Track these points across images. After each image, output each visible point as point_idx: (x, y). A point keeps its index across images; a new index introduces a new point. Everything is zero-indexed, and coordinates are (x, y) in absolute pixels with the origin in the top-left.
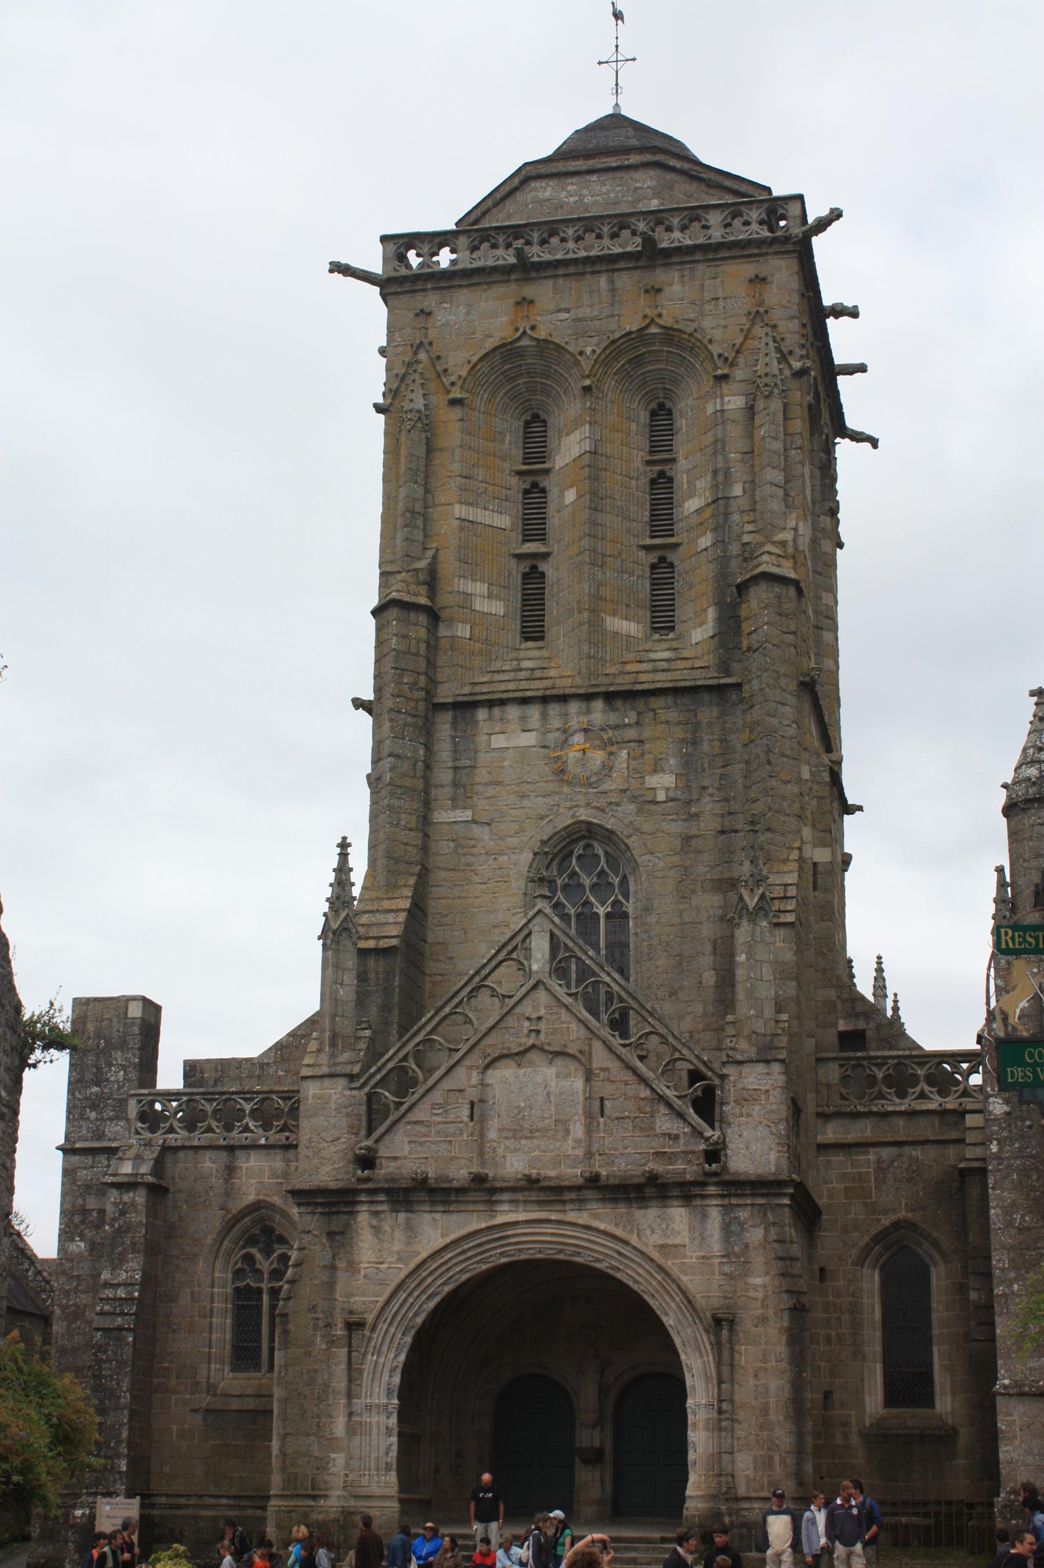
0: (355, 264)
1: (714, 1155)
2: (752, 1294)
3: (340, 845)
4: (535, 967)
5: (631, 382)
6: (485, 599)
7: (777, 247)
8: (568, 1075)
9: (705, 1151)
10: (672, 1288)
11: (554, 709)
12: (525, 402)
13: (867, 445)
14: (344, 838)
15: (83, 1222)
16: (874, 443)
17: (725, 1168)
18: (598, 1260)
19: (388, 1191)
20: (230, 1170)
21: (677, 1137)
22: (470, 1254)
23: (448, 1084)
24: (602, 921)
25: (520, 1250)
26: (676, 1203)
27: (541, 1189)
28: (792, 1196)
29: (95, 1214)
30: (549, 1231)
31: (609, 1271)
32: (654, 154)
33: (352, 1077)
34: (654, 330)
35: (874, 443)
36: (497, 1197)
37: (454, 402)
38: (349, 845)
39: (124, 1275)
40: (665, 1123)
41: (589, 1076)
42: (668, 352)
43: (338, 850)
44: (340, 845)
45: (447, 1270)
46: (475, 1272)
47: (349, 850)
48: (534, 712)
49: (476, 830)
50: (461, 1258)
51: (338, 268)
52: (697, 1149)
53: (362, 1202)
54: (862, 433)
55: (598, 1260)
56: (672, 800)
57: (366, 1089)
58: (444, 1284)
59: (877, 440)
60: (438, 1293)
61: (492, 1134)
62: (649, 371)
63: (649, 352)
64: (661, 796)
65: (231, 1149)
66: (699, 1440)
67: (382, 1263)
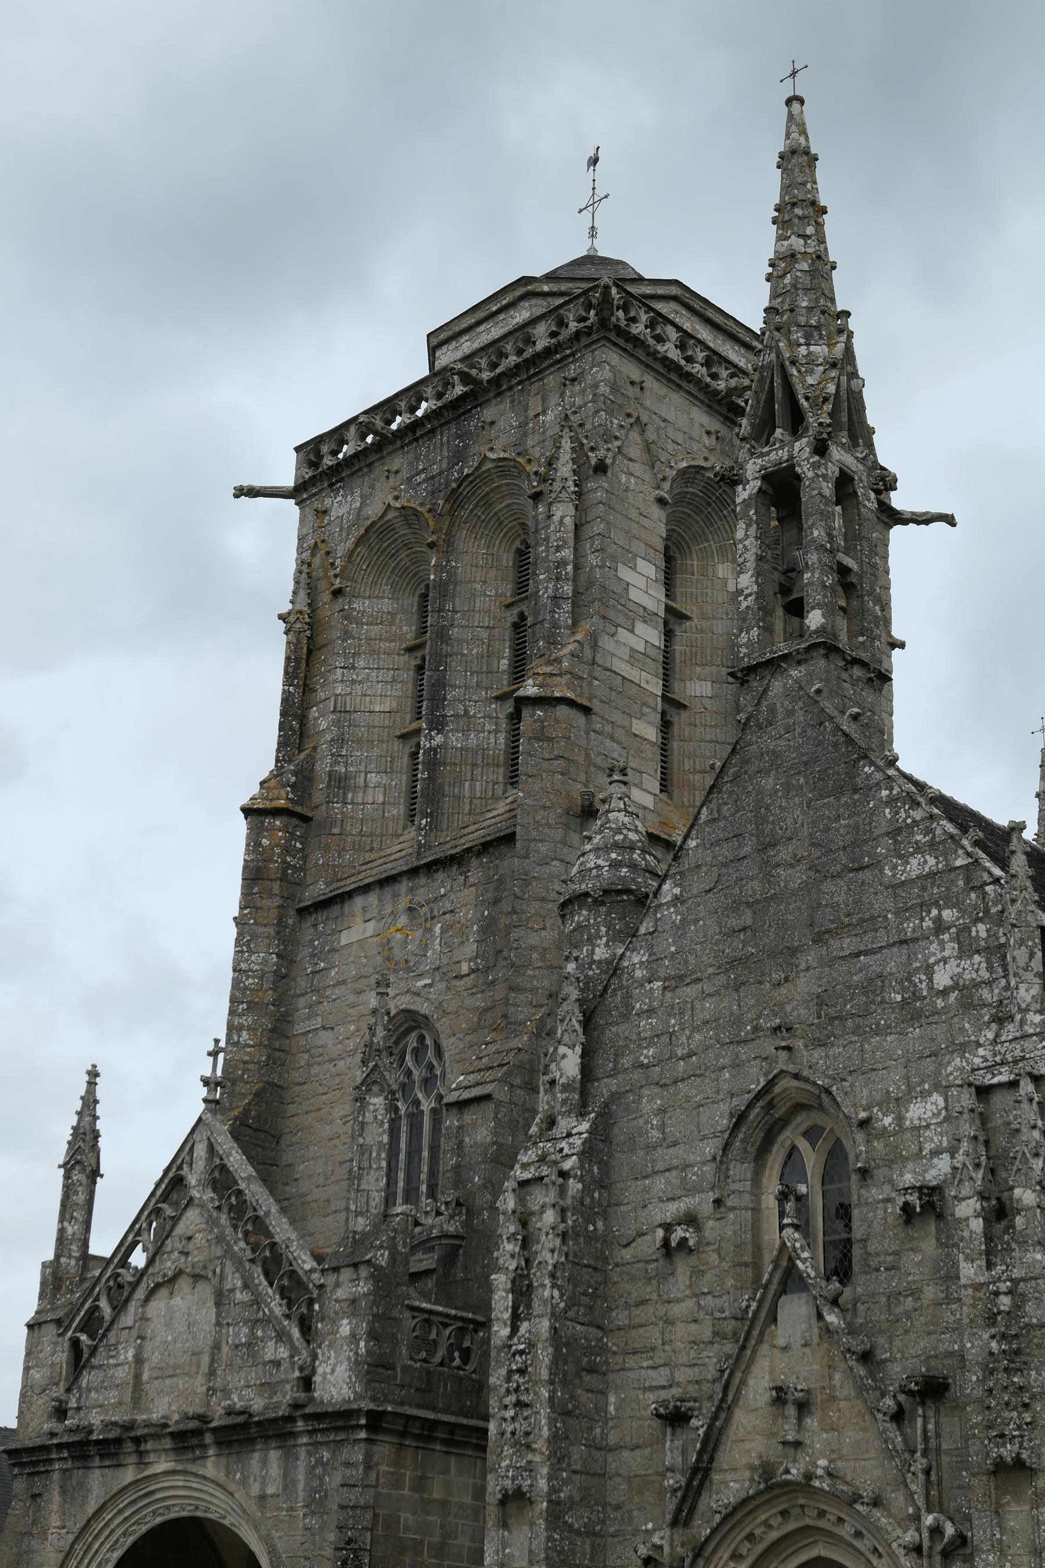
0: (258, 483)
1: (307, 1383)
3: (89, 1073)
5: (486, 527)
6: (377, 789)
7: (584, 341)
9: (299, 1378)
11: (388, 892)
12: (415, 574)
13: (942, 525)
14: (94, 1066)
16: (950, 520)
17: (311, 1400)
19: (67, 1445)
21: (277, 1363)
22: (127, 1514)
24: (426, 1118)
25: (168, 1508)
26: (274, 1445)
27: (172, 1435)
28: (368, 1427)
30: (180, 1484)
32: (526, 285)
33: (58, 1322)
34: (488, 466)
35: (950, 520)
36: (143, 1447)
37: (337, 593)
38: (97, 1075)
41: (221, 1298)
42: (508, 484)
43: (87, 1078)
44: (89, 1073)
45: (113, 1531)
46: (137, 1535)
47: (98, 1080)
48: (372, 898)
49: (326, 1037)
50: (120, 1518)
51: (241, 492)
52: (291, 1376)
53: (52, 1460)
54: (925, 514)
56: (474, 971)
57: (69, 1334)
58: (112, 1549)
59: (953, 516)
60: (108, 1561)
61: (145, 1377)
62: (500, 510)
63: (493, 490)
64: (465, 968)
67: (64, 1527)
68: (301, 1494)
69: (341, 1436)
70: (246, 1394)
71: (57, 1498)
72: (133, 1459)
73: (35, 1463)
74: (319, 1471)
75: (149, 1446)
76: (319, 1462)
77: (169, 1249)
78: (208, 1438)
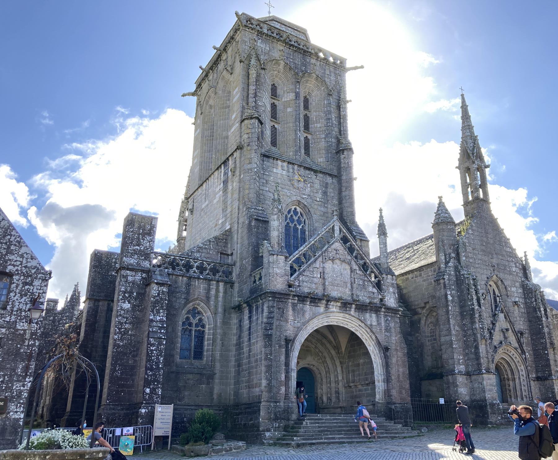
1: (381, 300)
2: (393, 342)
4: (336, 236)
8: (346, 270)
10: (374, 337)
15: (129, 296)
18: (353, 327)
19: (298, 296)
20: (188, 285)
21: (374, 293)
23: (314, 265)
29: (135, 294)
31: (354, 331)
36: (329, 303)
39: (158, 318)
40: (370, 289)
55: (353, 327)
57: (290, 262)
61: (327, 283)
65: (190, 278)
66: (380, 386)
68: (383, 327)
69: (393, 315)
70: (364, 298)
71: (290, 312)
72: (324, 305)
73: (279, 298)
74: (388, 322)
75: (332, 303)
76: (387, 320)
77: (330, 250)
78: (354, 306)
